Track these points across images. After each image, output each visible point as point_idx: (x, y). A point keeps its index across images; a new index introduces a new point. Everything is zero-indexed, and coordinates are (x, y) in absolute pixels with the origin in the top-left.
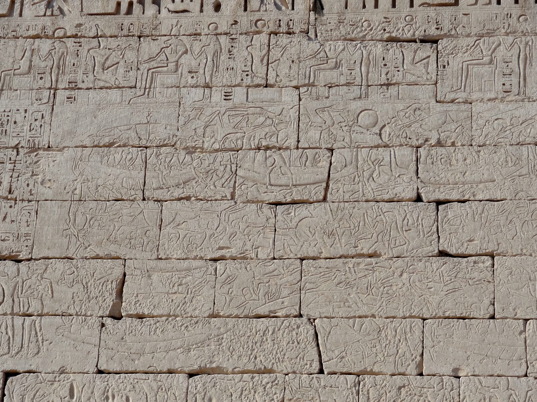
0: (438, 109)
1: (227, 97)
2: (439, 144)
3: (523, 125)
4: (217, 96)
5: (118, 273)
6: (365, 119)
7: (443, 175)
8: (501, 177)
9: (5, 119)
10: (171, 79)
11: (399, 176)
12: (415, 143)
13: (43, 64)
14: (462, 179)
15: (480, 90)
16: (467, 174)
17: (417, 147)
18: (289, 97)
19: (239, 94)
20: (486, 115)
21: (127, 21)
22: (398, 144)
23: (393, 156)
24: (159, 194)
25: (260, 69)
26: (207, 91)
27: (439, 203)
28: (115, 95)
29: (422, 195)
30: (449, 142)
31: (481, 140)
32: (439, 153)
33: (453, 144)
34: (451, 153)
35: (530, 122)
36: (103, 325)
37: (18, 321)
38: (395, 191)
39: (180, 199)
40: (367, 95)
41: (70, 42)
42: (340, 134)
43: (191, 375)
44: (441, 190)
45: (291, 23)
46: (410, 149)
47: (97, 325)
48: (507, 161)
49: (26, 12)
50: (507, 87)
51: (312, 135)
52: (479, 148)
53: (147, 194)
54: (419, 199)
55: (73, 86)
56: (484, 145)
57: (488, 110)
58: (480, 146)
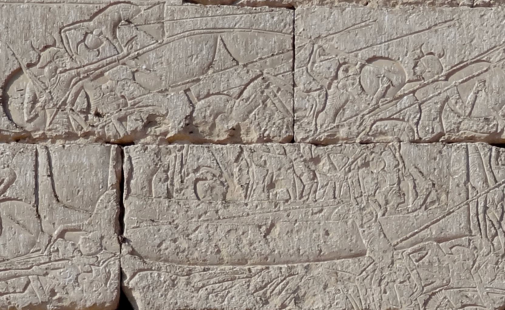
0: (189, 24)
2: (191, 133)
3: (455, 80)
7: (200, 234)
8: (381, 243)
11: (62, 235)
12: (114, 129)
14: (260, 247)
16: (276, 231)
17: (122, 144)
20: (340, 45)
22: (62, 130)
23: (42, 170)
29: (136, 295)
30: (222, 130)
31: (323, 126)
32: (191, 163)
33: (234, 136)
34: (228, 165)
35: (475, 69)
38: (48, 282)
44: (196, 279)
46: (98, 147)
48: (401, 194)
52: (317, 151)
56: (331, 140)
57: (346, 30)
58: (317, 144)
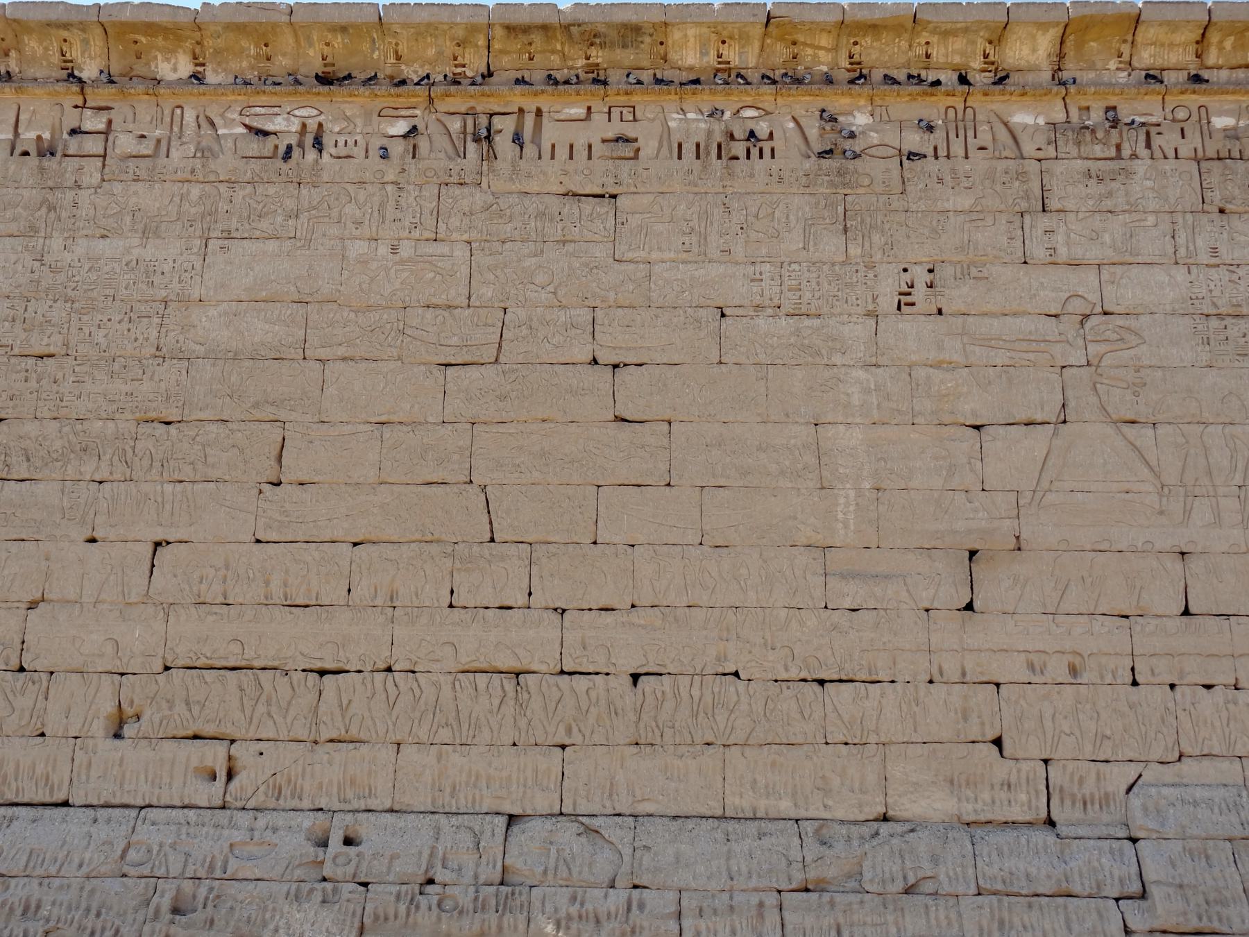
1: (394, 250)
4: (383, 250)
5: (275, 434)
6: (540, 278)
9: (151, 269)
10: (334, 231)
13: (193, 210)
15: (660, 249)
18: (461, 252)
19: (406, 250)
21: (285, 167)
24: (323, 353)
25: (430, 222)
26: (373, 244)
27: (615, 366)
28: (272, 246)
36: (261, 492)
37: (169, 488)
39: (344, 359)
40: (542, 251)
41: (223, 188)
42: (513, 291)
43: (355, 544)
45: (462, 173)
47: (256, 491)
49: (173, 150)
50: (687, 246)
51: (487, 292)
53: (308, 353)
54: (595, 361)
55: (228, 235)
